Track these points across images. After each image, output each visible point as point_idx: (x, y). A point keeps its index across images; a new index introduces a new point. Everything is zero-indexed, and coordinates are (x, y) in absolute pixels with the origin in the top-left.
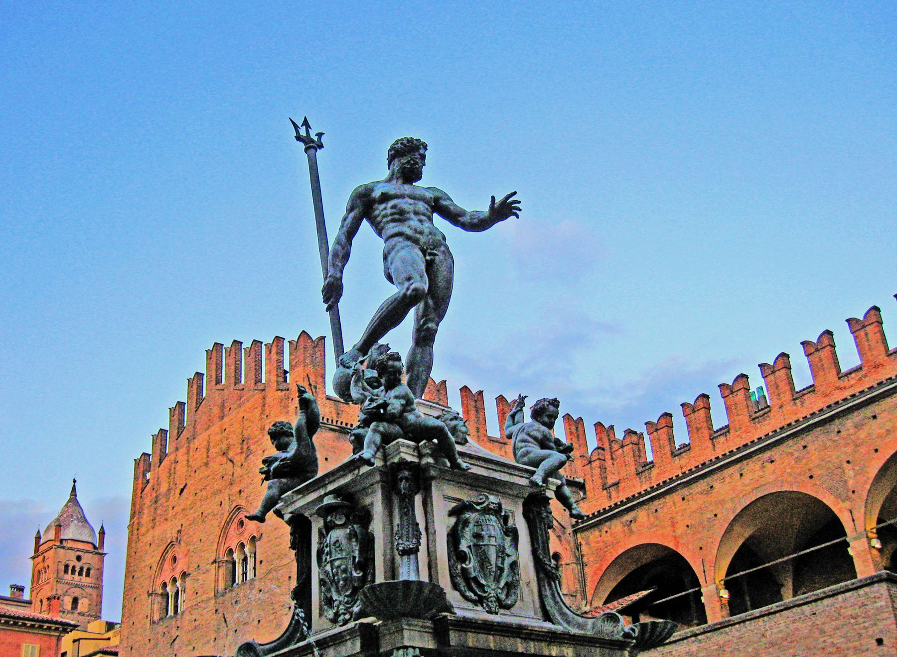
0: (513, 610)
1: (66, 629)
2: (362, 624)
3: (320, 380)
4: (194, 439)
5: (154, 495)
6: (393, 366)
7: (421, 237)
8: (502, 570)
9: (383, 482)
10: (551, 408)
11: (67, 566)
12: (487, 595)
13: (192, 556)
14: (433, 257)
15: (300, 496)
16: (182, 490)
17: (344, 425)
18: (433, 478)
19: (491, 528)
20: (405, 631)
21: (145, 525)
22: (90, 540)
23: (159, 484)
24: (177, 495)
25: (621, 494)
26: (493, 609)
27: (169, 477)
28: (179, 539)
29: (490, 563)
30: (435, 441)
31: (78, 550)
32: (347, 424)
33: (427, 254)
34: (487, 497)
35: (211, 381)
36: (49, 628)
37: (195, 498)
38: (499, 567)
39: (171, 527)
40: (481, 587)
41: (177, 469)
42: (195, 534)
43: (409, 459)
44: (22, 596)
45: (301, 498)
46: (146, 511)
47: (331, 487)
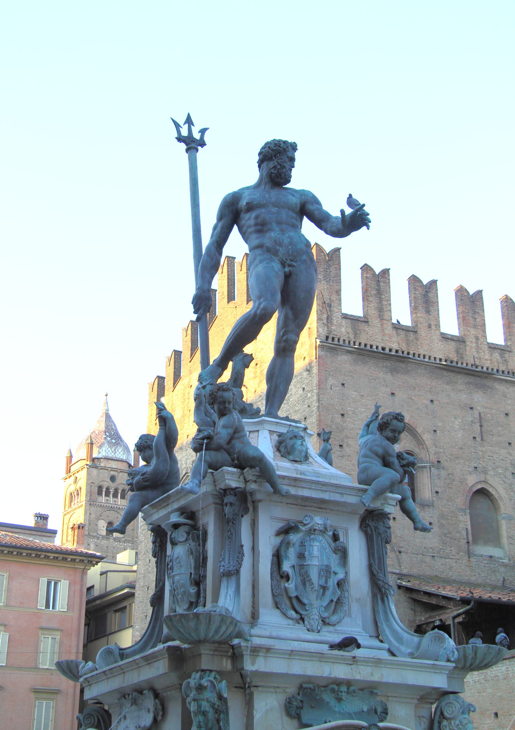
0: (338, 627)
1: (91, 562)
2: (169, 647)
3: (334, 297)
6: (222, 397)
7: (281, 249)
8: (324, 588)
9: (214, 503)
10: (395, 422)
11: (100, 488)
12: (308, 612)
14: (291, 268)
15: (155, 510)
17: (362, 346)
18: (260, 501)
19: (315, 549)
20: (203, 656)
22: (124, 457)
26: (315, 627)
30: (258, 468)
31: (113, 469)
32: (366, 345)
33: (286, 264)
34: (312, 518)
35: (223, 298)
36: (73, 560)
38: (321, 586)
39: (186, 457)
40: (303, 604)
43: (234, 485)
44: (47, 525)
45: (155, 512)
47: (176, 506)
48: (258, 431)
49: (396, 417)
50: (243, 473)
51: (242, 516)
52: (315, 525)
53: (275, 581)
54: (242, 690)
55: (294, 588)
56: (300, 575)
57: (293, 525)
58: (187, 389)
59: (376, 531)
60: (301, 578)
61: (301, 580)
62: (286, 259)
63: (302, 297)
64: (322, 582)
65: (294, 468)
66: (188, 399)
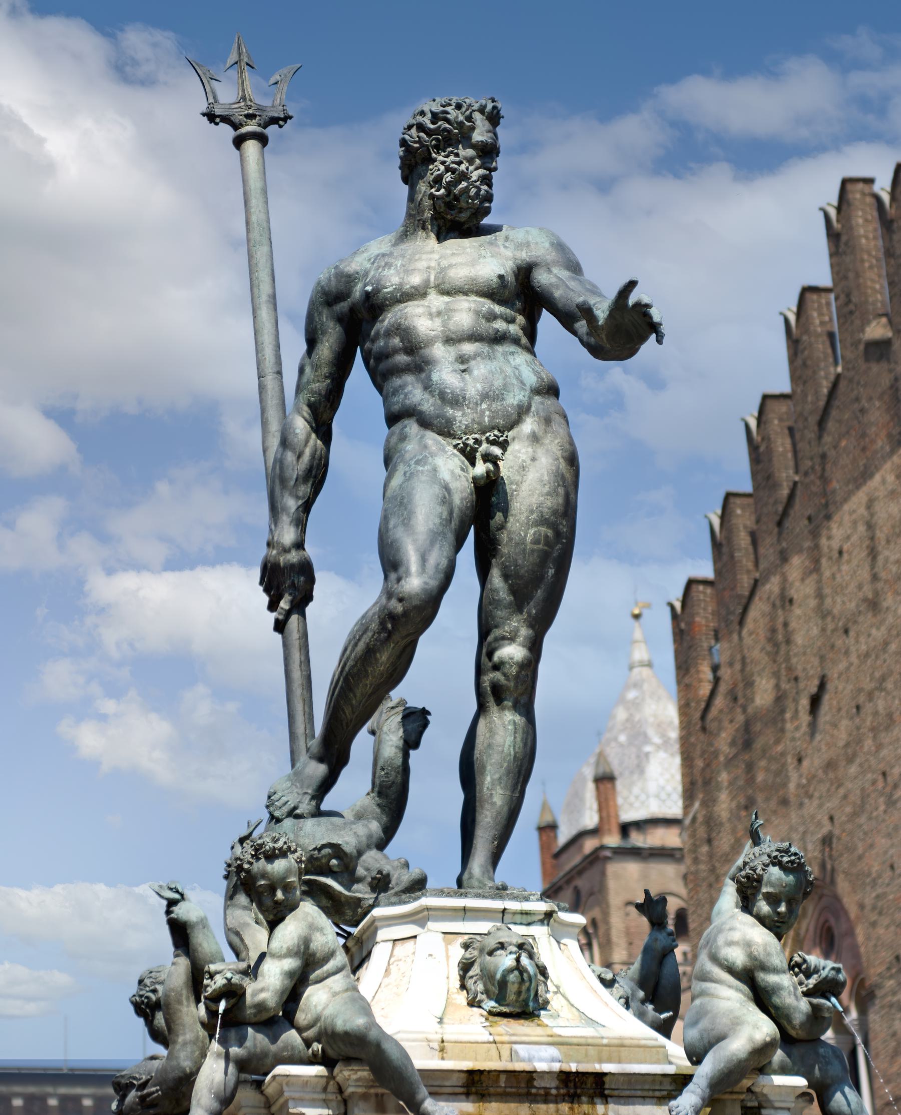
4: (828, 517)
5: (740, 718)
6: (264, 875)
7: (459, 414)
13: (874, 924)
16: (815, 702)
21: (727, 826)
23: (749, 684)
24: (805, 718)
27: (773, 656)
28: (829, 867)
33: (478, 455)
37: (857, 720)
39: (801, 829)
41: (793, 625)
42: (871, 846)
46: (724, 777)
48: (415, 937)
49: (776, 857)
58: (780, 612)
62: (476, 440)
63: (529, 538)
65: (491, 1039)
66: (788, 642)
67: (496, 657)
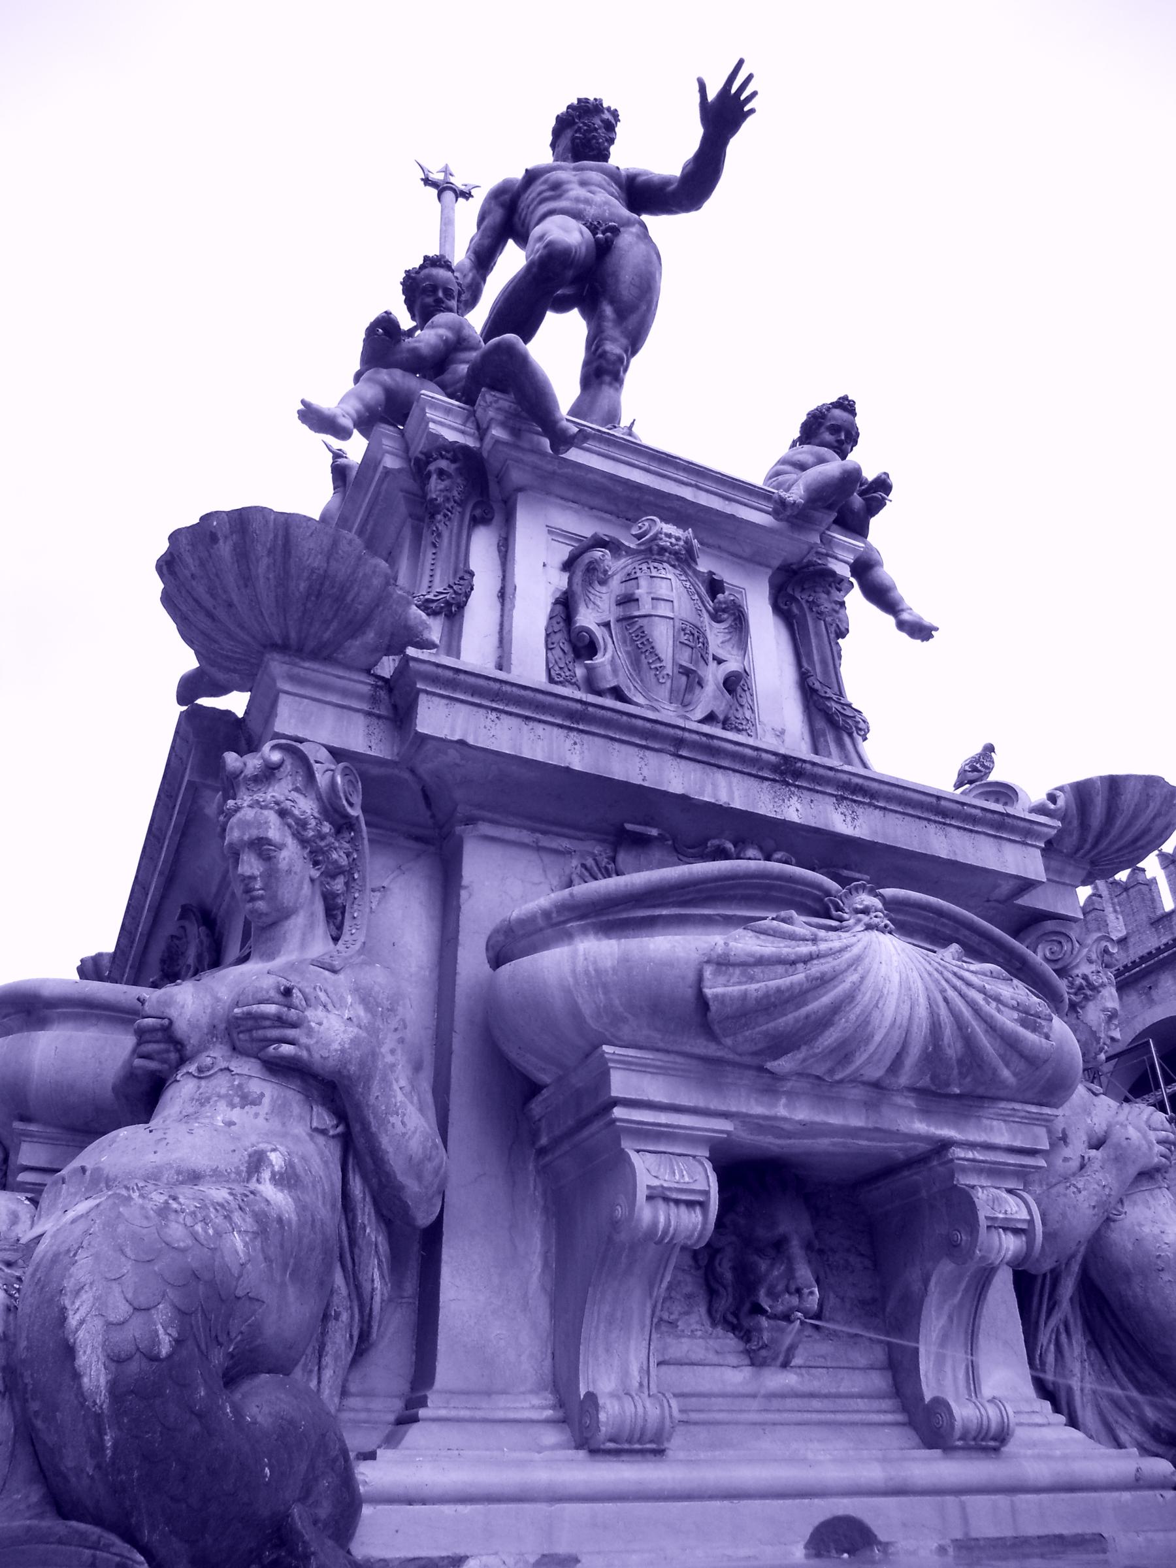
7: (588, 208)
8: (691, 678)
9: (410, 516)
18: (520, 489)
25: (1131, 951)
29: (656, 655)
38: (681, 666)
43: (451, 436)
50: (475, 411)
51: (476, 522)
52: (661, 539)
53: (557, 653)
54: (432, 849)
55: (609, 668)
56: (625, 642)
57: (607, 539)
59: (811, 610)
60: (629, 649)
61: (628, 653)
62: (599, 223)
64: (685, 658)
67: (600, 350)
